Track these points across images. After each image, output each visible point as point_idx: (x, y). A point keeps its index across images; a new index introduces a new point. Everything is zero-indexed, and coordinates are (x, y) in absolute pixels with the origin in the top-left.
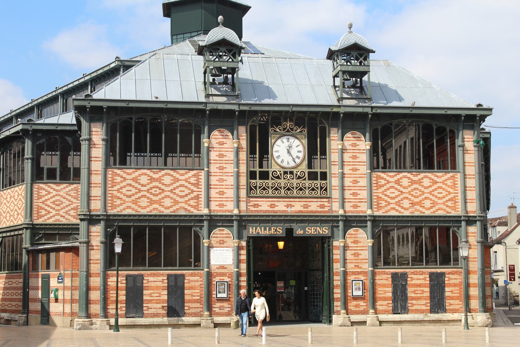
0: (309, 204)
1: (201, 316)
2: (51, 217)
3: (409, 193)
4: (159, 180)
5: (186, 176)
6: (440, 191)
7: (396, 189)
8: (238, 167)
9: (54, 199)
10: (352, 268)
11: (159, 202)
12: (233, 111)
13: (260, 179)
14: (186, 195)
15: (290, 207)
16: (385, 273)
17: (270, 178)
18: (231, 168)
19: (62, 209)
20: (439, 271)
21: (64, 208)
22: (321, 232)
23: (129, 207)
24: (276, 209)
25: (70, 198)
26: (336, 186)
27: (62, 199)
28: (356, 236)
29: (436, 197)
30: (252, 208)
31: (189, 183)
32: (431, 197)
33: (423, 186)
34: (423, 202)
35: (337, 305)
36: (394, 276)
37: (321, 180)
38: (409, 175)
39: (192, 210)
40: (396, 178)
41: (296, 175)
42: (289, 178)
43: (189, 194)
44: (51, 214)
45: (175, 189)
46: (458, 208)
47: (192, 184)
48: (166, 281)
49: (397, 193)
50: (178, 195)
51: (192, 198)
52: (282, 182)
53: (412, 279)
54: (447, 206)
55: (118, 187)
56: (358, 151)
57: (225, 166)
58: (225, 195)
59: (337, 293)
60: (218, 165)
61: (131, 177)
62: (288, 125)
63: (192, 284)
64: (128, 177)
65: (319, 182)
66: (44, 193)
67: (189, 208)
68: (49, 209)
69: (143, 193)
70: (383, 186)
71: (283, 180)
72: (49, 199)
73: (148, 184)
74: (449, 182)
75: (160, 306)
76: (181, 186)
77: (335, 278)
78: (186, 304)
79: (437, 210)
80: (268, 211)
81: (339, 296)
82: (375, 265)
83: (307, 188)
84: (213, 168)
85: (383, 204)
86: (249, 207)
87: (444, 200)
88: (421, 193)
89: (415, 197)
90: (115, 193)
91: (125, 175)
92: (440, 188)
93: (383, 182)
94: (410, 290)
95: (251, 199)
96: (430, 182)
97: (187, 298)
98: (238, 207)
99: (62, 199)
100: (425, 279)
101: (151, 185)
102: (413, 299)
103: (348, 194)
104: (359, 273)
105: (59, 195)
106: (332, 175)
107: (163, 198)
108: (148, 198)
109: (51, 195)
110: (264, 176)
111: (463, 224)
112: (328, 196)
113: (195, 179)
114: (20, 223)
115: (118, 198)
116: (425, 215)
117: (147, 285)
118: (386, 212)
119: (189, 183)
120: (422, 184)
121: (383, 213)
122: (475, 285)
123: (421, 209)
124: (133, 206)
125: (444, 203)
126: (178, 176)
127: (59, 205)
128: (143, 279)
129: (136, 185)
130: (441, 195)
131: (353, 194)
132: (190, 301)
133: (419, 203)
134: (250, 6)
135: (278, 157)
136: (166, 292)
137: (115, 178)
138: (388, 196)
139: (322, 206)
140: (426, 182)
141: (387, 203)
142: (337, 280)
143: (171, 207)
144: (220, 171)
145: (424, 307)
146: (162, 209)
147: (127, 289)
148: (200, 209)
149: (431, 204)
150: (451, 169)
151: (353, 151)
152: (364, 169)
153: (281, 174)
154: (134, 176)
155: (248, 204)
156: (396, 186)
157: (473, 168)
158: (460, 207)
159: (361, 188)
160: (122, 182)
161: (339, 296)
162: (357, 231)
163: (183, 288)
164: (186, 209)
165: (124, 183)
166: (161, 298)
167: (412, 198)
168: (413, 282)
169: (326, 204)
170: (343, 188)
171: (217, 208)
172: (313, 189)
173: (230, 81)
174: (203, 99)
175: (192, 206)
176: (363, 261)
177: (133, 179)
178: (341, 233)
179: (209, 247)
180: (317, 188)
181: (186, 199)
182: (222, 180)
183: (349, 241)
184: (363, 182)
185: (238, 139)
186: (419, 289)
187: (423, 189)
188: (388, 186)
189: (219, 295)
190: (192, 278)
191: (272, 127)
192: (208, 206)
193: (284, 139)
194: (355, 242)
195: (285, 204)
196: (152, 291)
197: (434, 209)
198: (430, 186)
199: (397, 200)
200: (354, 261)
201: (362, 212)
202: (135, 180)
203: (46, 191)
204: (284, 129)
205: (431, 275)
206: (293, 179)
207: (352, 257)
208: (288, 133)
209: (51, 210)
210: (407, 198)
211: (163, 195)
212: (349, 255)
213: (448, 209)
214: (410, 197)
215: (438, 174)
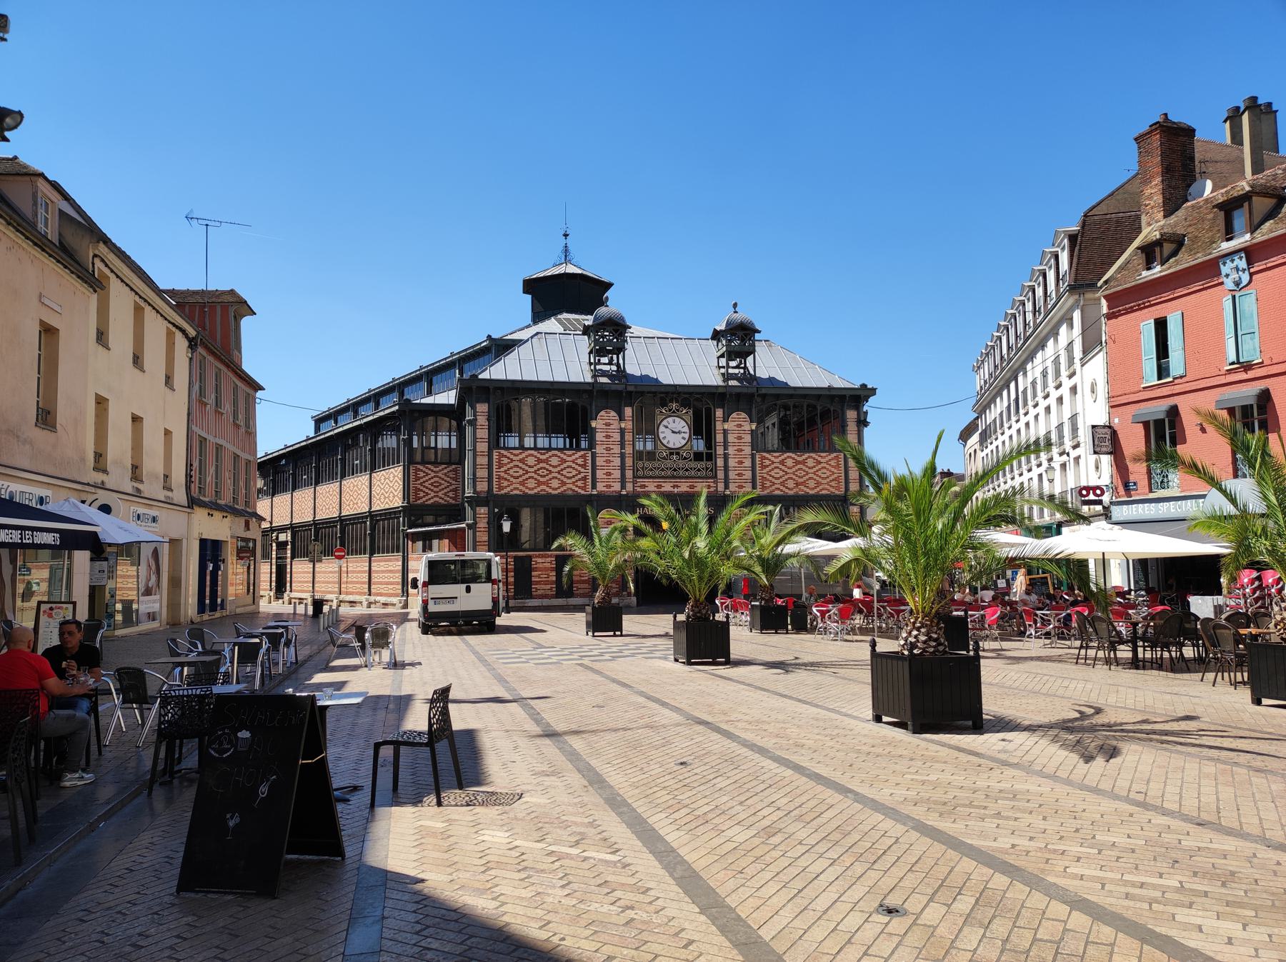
0: (695, 484)
2: (430, 499)
3: (794, 473)
4: (546, 461)
5: (574, 457)
6: (824, 471)
7: (781, 469)
8: (623, 447)
9: (432, 481)
11: (546, 484)
14: (574, 476)
18: (617, 449)
19: (440, 490)
21: (443, 489)
23: (517, 489)
25: (448, 479)
27: (441, 481)
30: (639, 489)
31: (577, 464)
32: (815, 477)
33: (807, 467)
38: (793, 455)
40: (780, 458)
43: (577, 475)
44: (430, 496)
45: (562, 470)
47: (579, 465)
48: (554, 562)
50: (565, 476)
54: (831, 486)
55: (505, 468)
57: (612, 447)
61: (518, 458)
64: (515, 458)
66: (422, 474)
67: (576, 489)
68: (427, 491)
69: (529, 475)
70: (767, 466)
72: (427, 481)
74: (832, 463)
75: (549, 587)
76: (568, 467)
79: (821, 490)
85: (768, 484)
87: (828, 480)
89: (799, 477)
90: (502, 474)
91: (512, 457)
93: (767, 462)
98: (623, 487)
99: (441, 481)
101: (538, 466)
103: (732, 475)
105: (437, 477)
108: (536, 479)
109: (430, 477)
114: (396, 505)
115: (506, 479)
119: (577, 464)
123: (805, 489)
124: (521, 487)
125: (828, 484)
126: (565, 457)
127: (437, 487)
128: (531, 561)
129: (524, 466)
131: (738, 475)
132: (578, 582)
133: (803, 483)
134: (612, 281)
135: (664, 438)
138: (773, 477)
140: (810, 463)
146: (550, 491)
147: (515, 570)
152: (748, 450)
154: (521, 457)
156: (781, 466)
165: (512, 465)
166: (551, 579)
169: (712, 484)
171: (605, 489)
172: (699, 470)
173: (615, 361)
174: (589, 379)
175: (579, 487)
177: (520, 461)
181: (573, 480)
184: (748, 463)
187: (807, 469)
188: (773, 466)
192: (594, 486)
193: (670, 419)
199: (781, 480)
202: (522, 461)
203: (424, 472)
204: (670, 410)
208: (673, 413)
209: (430, 492)
210: (791, 478)
211: (550, 476)
214: (794, 477)
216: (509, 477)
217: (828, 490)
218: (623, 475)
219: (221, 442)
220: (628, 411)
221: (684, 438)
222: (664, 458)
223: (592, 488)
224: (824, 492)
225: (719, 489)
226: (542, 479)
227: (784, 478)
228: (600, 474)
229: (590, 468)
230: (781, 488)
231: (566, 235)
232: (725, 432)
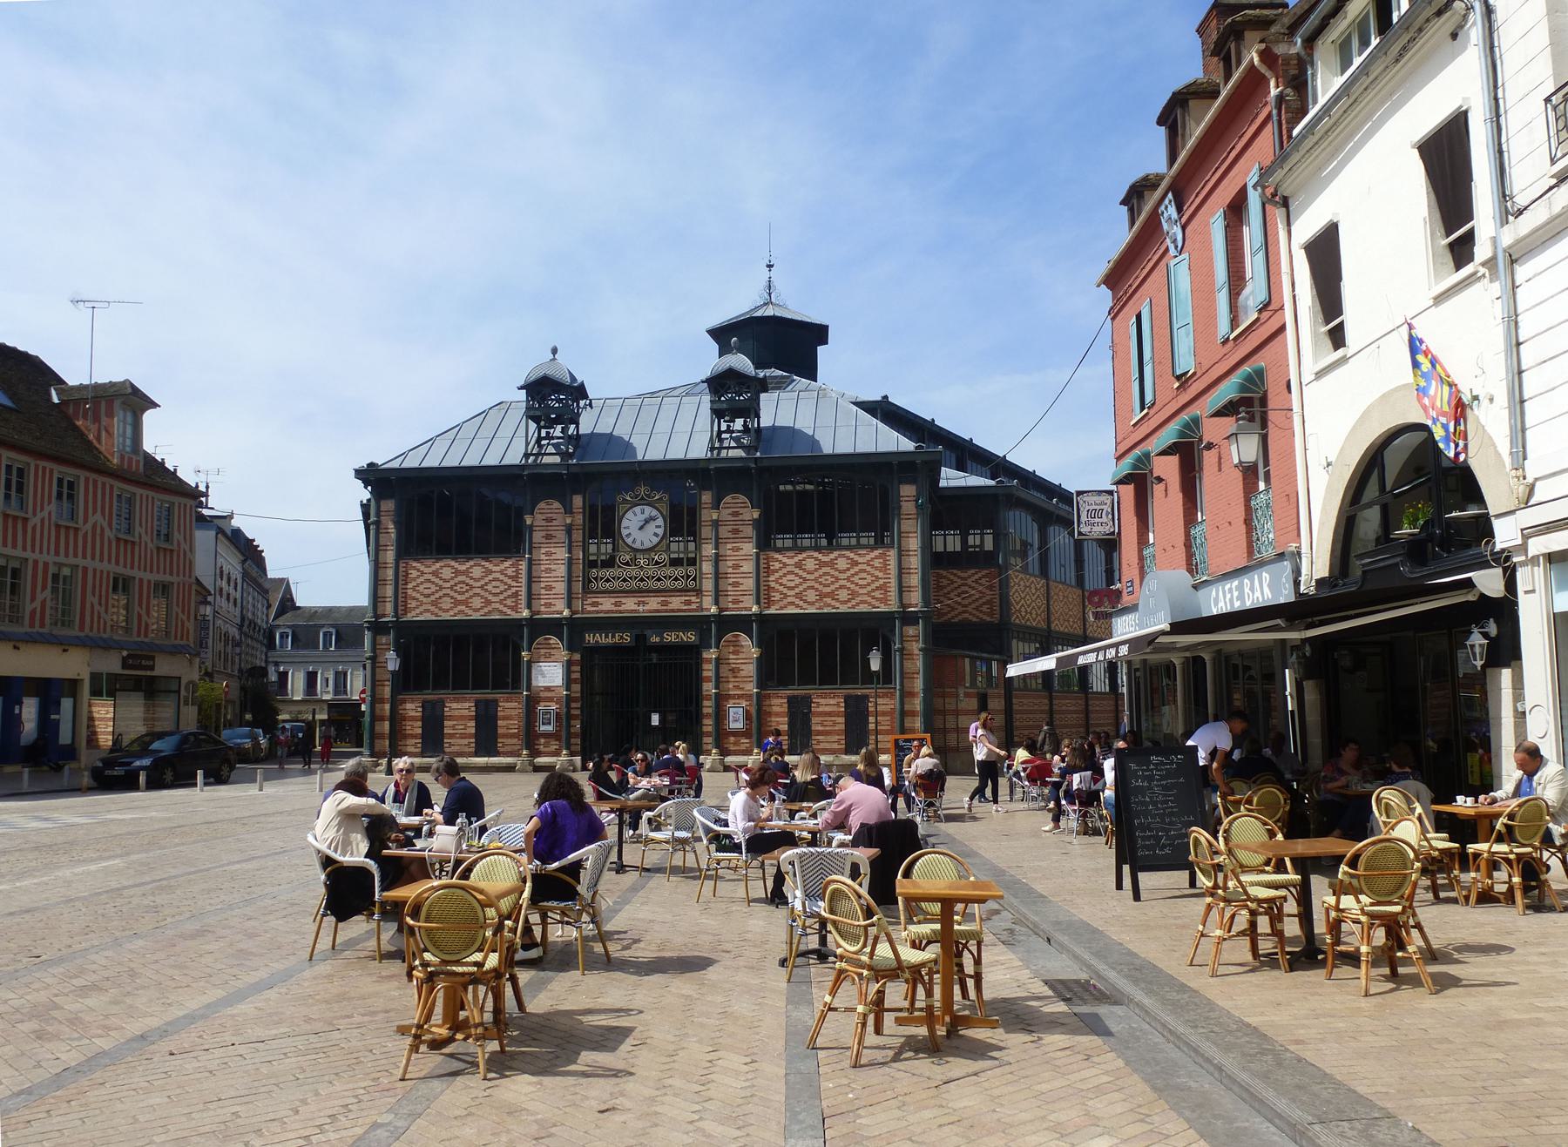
1: (519, 756)
3: (816, 580)
4: (466, 573)
6: (864, 575)
7: (797, 575)
11: (466, 603)
12: (561, 475)
14: (501, 592)
20: (859, 692)
29: (857, 584)
30: (589, 608)
32: (848, 584)
33: (836, 570)
35: (708, 741)
36: (792, 701)
39: (509, 612)
40: (796, 559)
43: (506, 590)
45: (486, 584)
47: (510, 577)
48: (473, 709)
49: (798, 581)
50: (490, 593)
51: (509, 597)
54: (873, 598)
55: (414, 584)
59: (708, 725)
61: (430, 570)
63: (508, 712)
64: (426, 570)
67: (505, 609)
69: (444, 591)
73: (452, 578)
74: (877, 563)
76: (495, 580)
77: (706, 703)
78: (499, 740)
79: (858, 604)
80: (612, 612)
81: (710, 729)
82: (762, 684)
85: (777, 596)
87: (869, 589)
92: (864, 571)
94: (814, 720)
97: (500, 731)
100: (838, 705)
101: (456, 580)
102: (819, 733)
107: (471, 597)
108: (452, 597)
117: (449, 714)
123: (833, 603)
124: (433, 608)
129: (437, 581)
133: (831, 595)
136: (473, 724)
139: (689, 603)
142: (708, 707)
143: (482, 608)
145: (836, 746)
146: (470, 612)
154: (434, 568)
156: (797, 570)
159: (745, 575)
161: (710, 729)
163: (495, 718)
164: (501, 612)
165: (422, 579)
167: (820, 587)
168: (820, 709)
169: (693, 599)
175: (509, 607)
179: (530, 663)
180: (682, 577)
181: (502, 597)
184: (748, 567)
185: (571, 513)
187: (836, 574)
188: (785, 571)
189: (543, 728)
190: (508, 705)
193: (638, 509)
195: (636, 600)
198: (848, 569)
199: (797, 590)
201: (746, 609)
202: (435, 574)
205: (847, 699)
210: (812, 588)
211: (471, 593)
213: (874, 602)
214: (816, 585)
216: (418, 596)
220: (578, 501)
222: (627, 564)
224: (863, 608)
225: (705, 606)
226: (459, 597)
227: (801, 588)
230: (797, 601)
231: (770, 266)
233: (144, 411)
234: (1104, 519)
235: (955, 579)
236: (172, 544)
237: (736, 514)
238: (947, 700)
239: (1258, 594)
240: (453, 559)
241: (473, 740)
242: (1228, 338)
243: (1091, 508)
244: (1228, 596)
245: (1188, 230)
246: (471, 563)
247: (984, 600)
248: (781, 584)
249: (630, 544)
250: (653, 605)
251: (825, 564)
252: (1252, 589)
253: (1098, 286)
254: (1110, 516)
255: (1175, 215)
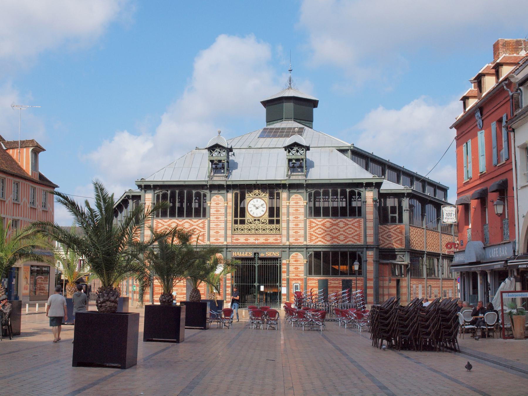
0: (268, 238)
5: (197, 223)
6: (350, 229)
10: (294, 276)
13: (240, 224)
15: (257, 240)
16: (314, 279)
17: (246, 223)
18: (222, 218)
20: (348, 278)
22: (275, 255)
24: (249, 241)
26: (284, 228)
28: (297, 257)
29: (347, 233)
30: (235, 241)
32: (344, 233)
33: (339, 227)
34: (339, 237)
37: (276, 224)
41: (262, 221)
42: (257, 223)
46: (361, 240)
47: (201, 227)
52: (253, 226)
53: (331, 283)
54: (354, 239)
56: (299, 206)
57: (219, 217)
58: (219, 234)
60: (215, 217)
62: (257, 192)
64: (165, 224)
65: (274, 226)
70: (314, 227)
71: (253, 224)
74: (356, 224)
79: (348, 242)
83: (268, 229)
84: (212, 218)
86: (233, 241)
87: (353, 235)
88: (338, 231)
89: (334, 233)
91: (163, 223)
92: (350, 228)
93: (314, 225)
95: (234, 236)
96: (344, 225)
98: (226, 240)
103: (291, 232)
104: (298, 279)
106: (283, 221)
110: (243, 222)
111: (365, 249)
112: (280, 233)
113: (203, 224)
116: (340, 244)
118: (316, 243)
119: (199, 227)
120: (339, 226)
121: (314, 243)
122: (371, 288)
125: (352, 237)
126: (192, 223)
130: (351, 232)
131: (296, 232)
133: (337, 238)
134: (318, 100)
135: (251, 211)
136: (185, 289)
137: (158, 224)
139: (277, 240)
141: (316, 238)
144: (217, 220)
148: (205, 242)
149: (344, 237)
150: (358, 216)
151: (296, 207)
152: (302, 217)
153: (252, 221)
154: (168, 223)
155: (233, 239)
157: (372, 216)
158: (363, 239)
160: (162, 227)
162: (297, 254)
167: (332, 234)
168: (332, 285)
169: (279, 238)
170: (288, 228)
171: (215, 241)
174: (207, 179)
176: (300, 272)
178: (288, 256)
180: (274, 229)
182: (218, 225)
183: (292, 261)
184: (302, 225)
185: (227, 201)
186: (335, 289)
187: (339, 229)
188: (317, 227)
191: (248, 193)
192: (209, 240)
193: (255, 200)
194: (296, 261)
195: (254, 238)
196: (177, 288)
197: (346, 241)
198: (344, 227)
200: (295, 272)
205: (343, 281)
206: (259, 224)
207: (294, 270)
212: (291, 268)
213: (355, 241)
215: (349, 219)
217: (353, 241)
218: (226, 233)
219: (15, 217)
221: (263, 211)
222: (250, 223)
223: (208, 241)
224: (350, 243)
228: (212, 232)
229: (207, 229)
232: (288, 207)
233: (39, 152)
234: (453, 217)
235: (386, 229)
236: (47, 209)
237: (297, 203)
238: (384, 282)
239: (503, 253)
240: (177, 219)
241: (185, 296)
242: (496, 165)
243: (448, 212)
244: (495, 252)
245: (484, 122)
246: (184, 221)
247: (398, 238)
248: (316, 233)
249: (252, 214)
250: (261, 240)
251: (334, 225)
252: (502, 251)
253: (451, 128)
254: (455, 216)
255: (480, 116)
